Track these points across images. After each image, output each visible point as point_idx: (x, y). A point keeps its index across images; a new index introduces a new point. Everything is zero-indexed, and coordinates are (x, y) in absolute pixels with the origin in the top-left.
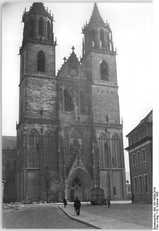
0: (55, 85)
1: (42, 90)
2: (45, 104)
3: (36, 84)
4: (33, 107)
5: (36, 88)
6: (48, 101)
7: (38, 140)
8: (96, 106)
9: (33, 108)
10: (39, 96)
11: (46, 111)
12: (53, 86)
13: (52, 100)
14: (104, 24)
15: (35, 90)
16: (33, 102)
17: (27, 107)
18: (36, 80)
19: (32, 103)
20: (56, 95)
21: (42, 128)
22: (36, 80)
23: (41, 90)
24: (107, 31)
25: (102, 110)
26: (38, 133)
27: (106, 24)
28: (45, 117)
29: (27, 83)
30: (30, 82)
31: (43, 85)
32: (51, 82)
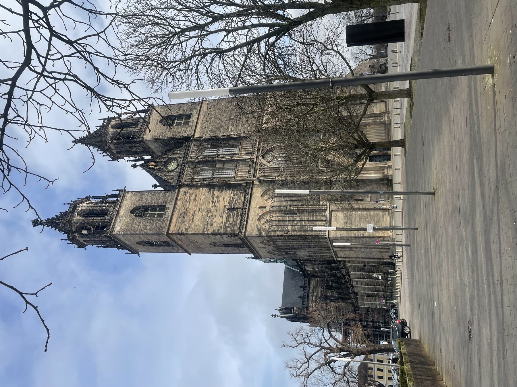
3: (184, 218)
6: (214, 201)
8: (229, 130)
9: (224, 222)
10: (205, 213)
11: (230, 202)
12: (191, 192)
13: (213, 193)
15: (193, 218)
16: (213, 222)
17: (220, 232)
19: (215, 225)
20: (204, 189)
26: (267, 213)
28: (239, 204)
29: (180, 232)
30: (179, 228)
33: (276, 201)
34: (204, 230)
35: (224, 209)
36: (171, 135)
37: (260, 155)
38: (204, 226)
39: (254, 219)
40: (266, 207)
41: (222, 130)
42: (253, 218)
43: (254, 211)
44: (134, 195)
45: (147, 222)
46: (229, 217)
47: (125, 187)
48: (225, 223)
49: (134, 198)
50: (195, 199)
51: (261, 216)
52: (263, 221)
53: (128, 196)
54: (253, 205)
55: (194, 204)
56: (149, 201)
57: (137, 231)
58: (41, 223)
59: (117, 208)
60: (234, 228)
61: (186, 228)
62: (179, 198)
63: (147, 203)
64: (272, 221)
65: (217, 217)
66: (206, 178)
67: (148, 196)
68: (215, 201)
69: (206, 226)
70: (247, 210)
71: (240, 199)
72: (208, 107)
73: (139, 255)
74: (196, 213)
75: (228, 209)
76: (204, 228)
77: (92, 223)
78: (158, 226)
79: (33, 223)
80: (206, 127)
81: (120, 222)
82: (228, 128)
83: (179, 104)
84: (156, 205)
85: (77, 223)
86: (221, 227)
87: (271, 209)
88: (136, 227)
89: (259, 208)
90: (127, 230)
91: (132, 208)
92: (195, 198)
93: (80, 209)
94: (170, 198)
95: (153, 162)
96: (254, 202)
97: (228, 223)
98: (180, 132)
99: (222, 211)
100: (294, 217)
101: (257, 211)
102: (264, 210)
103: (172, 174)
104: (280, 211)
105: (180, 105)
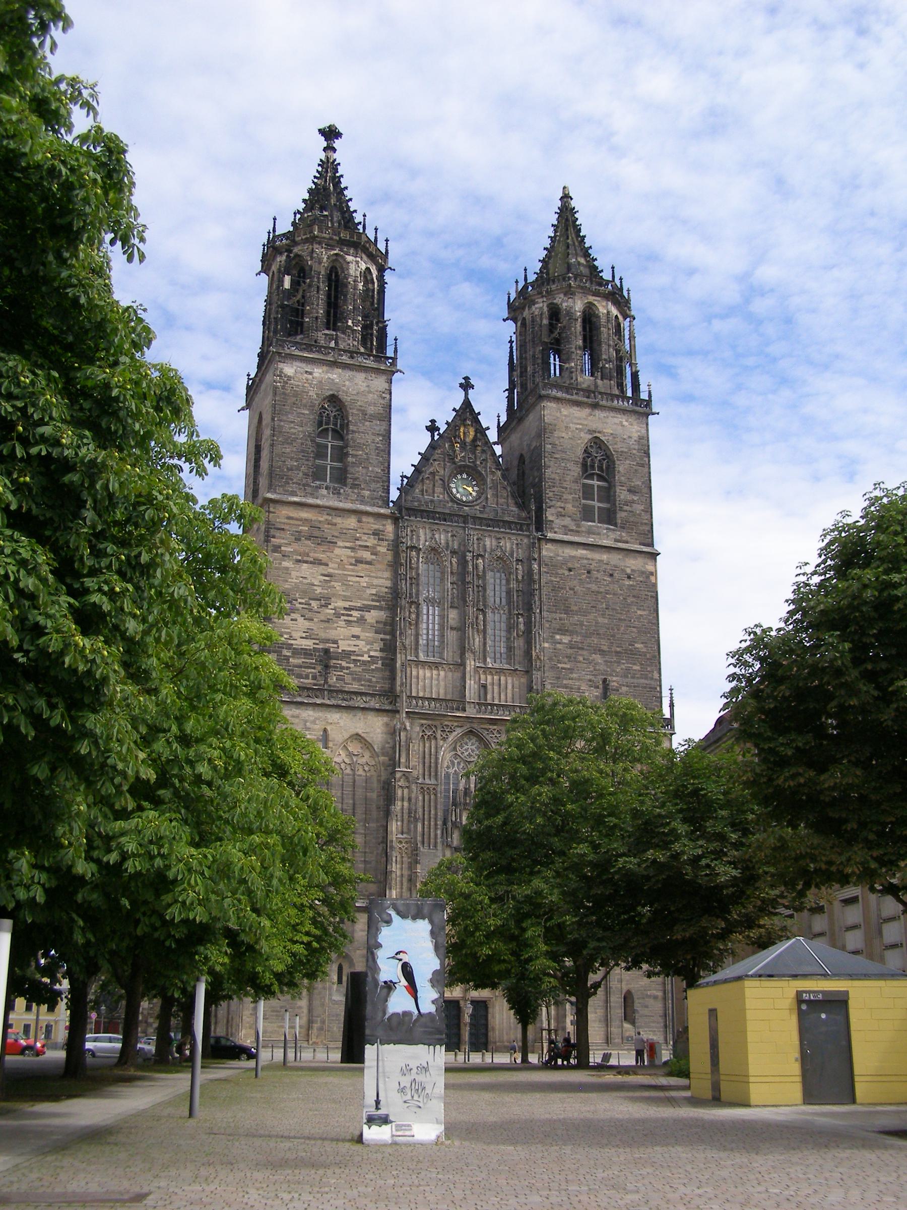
1: (331, 565)
2: (342, 623)
3: (309, 538)
4: (291, 638)
5: (308, 556)
6: (352, 613)
8: (558, 637)
9: (292, 642)
10: (319, 590)
11: (347, 655)
12: (379, 548)
13: (375, 608)
14: (602, 282)
15: (306, 562)
16: (294, 616)
18: (306, 520)
20: (388, 583)
21: (329, 728)
22: (305, 521)
23: (327, 565)
24: (615, 312)
25: (580, 652)
27: (608, 282)
29: (272, 532)
30: (283, 529)
35: (327, 641)
36: (553, 476)
37: (475, 726)
39: (296, 721)
41: (558, 616)
42: (297, 717)
43: (316, 719)
45: (302, 444)
46: (305, 654)
50: (359, 561)
53: (379, 383)
54: (334, 717)
55: (345, 562)
57: (281, 421)
58: (329, 148)
59: (345, 358)
61: (280, 547)
62: (364, 519)
65: (307, 624)
67: (373, 434)
68: (351, 616)
70: (319, 701)
72: (632, 570)
73: (243, 409)
74: (322, 569)
75: (326, 651)
79: (329, 127)
80: (570, 570)
81: (306, 372)
82: (563, 631)
90: (284, 394)
91: (345, 398)
92: (361, 562)
93: (349, 258)
94: (367, 493)
95: (476, 435)
97: (288, 654)
99: (323, 635)
102: (320, 745)
103: (438, 490)
105: (645, 490)
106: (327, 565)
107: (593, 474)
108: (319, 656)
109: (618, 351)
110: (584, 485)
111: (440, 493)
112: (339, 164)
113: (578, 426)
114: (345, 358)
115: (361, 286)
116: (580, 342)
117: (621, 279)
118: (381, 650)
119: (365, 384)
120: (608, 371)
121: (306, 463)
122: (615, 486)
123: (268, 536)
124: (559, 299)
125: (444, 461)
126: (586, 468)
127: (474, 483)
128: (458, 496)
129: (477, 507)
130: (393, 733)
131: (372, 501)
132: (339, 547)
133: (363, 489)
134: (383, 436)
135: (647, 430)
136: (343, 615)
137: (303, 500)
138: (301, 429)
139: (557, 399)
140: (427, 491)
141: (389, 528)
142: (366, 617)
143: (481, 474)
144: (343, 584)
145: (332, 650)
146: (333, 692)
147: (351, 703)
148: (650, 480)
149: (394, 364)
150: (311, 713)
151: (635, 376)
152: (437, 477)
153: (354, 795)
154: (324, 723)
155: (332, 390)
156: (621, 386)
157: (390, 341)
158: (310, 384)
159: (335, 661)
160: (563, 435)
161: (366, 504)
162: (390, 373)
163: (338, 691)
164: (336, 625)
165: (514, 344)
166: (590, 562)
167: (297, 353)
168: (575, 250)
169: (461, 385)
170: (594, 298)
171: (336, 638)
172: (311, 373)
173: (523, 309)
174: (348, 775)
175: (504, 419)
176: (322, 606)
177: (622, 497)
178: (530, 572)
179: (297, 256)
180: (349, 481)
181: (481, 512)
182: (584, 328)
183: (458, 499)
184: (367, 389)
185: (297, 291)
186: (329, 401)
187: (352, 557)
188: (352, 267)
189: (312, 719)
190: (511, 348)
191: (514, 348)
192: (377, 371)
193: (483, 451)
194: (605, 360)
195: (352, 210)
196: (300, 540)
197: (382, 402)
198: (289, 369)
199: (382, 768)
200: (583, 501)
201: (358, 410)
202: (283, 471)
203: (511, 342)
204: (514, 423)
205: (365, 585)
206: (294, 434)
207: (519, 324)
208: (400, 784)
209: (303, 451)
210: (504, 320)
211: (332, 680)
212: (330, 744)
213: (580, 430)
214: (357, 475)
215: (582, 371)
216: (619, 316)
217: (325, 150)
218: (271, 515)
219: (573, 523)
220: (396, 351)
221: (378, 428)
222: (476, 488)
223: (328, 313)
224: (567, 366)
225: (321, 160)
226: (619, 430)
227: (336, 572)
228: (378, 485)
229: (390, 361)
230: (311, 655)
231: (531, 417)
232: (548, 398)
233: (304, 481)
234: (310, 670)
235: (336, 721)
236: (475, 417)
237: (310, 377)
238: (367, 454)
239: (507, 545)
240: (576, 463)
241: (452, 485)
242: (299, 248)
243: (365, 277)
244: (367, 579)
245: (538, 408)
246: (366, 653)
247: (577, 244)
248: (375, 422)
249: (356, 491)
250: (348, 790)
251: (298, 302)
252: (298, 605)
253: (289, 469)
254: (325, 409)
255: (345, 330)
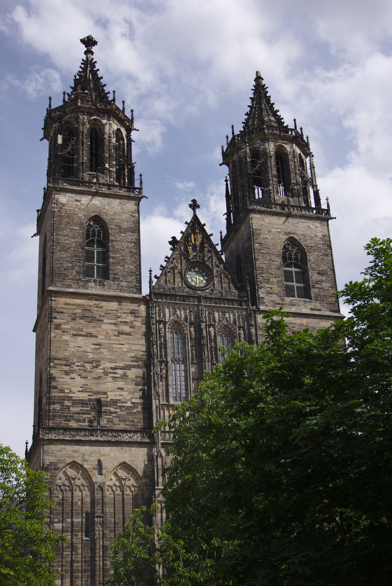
0: (140, 319)
1: (100, 337)
3: (83, 317)
5: (82, 330)
7: (88, 500)
10: (91, 356)
11: (114, 402)
12: (135, 323)
13: (134, 367)
14: (286, 129)
15: (81, 335)
16: (72, 375)
17: (53, 390)
18: (79, 305)
19: (67, 379)
20: (144, 348)
21: (102, 459)
23: (97, 337)
24: (298, 151)
27: (292, 130)
28: (110, 421)
29: (54, 315)
30: (62, 312)
31: (103, 321)
32: (129, 312)
33: (114, 494)
34: (56, 359)
35: (98, 393)
36: (261, 266)
38: (64, 359)
39: (77, 454)
40: (100, 473)
42: (77, 452)
43: (92, 452)
44: (132, 216)
45: (75, 251)
47: (145, 197)
48: (70, 399)
49: (124, 216)
50: (120, 333)
51: (82, 466)
52: (71, 472)
53: (131, 205)
55: (110, 333)
56: (117, 245)
57: (58, 235)
58: (88, 52)
59: (104, 190)
60: (60, 416)
61: (60, 325)
63: (115, 243)
64: (72, 491)
65: (83, 381)
66: (166, 348)
67: (127, 242)
68: (116, 373)
69: (64, 362)
70: (93, 438)
71: (120, 421)
73: (35, 235)
74: (93, 340)
75: (99, 401)
76: (60, 359)
77: (78, 149)
78: (66, 272)
79: (88, 37)
81: (76, 200)
83: (334, 270)
84: (111, 260)
85: (78, 122)
86: (62, 391)
87: (96, 486)
88: (66, 232)
89: (99, 461)
90: (60, 216)
91: (106, 218)
93: (104, 121)
94: (124, 284)
95: (203, 240)
96: (111, 451)
98: (268, 282)
99: (95, 389)
100: (80, 534)
101: (92, 458)
102: (96, 472)
103: (178, 280)
104: (93, 503)
105: (331, 273)
106: (97, 337)
107: (291, 263)
108: (93, 404)
109: (303, 177)
110: (285, 271)
111: (179, 282)
112: (96, 62)
113: (278, 230)
114: (104, 190)
115: (114, 140)
116: (275, 172)
117: (301, 129)
118: (140, 398)
119: (120, 207)
120: (296, 191)
121: (78, 264)
122: (308, 271)
123: (51, 318)
124: (258, 144)
125: (181, 259)
126: (286, 260)
127: (204, 274)
128: (193, 284)
129: (207, 291)
130: (151, 459)
131: (129, 289)
132: (105, 323)
133: (122, 281)
134: (135, 243)
135: (328, 231)
136: (110, 373)
137: (77, 290)
138: (73, 240)
139: (261, 212)
140: (169, 281)
141: (143, 308)
142: (128, 374)
143: (208, 267)
144: (109, 351)
145: (102, 399)
146: (103, 431)
147: (119, 439)
148: (333, 265)
149: (140, 192)
150: (87, 448)
151: (316, 194)
152: (176, 271)
153: (123, 510)
154: (98, 455)
155: (95, 212)
156: (307, 201)
157: (137, 177)
158: (79, 209)
159: (105, 408)
160: (267, 236)
161: (124, 291)
162: (138, 200)
163: (109, 431)
164: (105, 381)
165: (229, 182)
166: (294, 325)
167: (68, 187)
168: (267, 112)
169: (190, 206)
170: (283, 141)
171: (106, 391)
172: (79, 201)
173: (233, 155)
174: (118, 495)
175: (225, 233)
176: (94, 367)
177: (314, 278)
178: (250, 334)
179: (67, 122)
180: (111, 276)
181: (210, 294)
182: (277, 163)
183: (192, 286)
184: (121, 210)
185: (68, 145)
186: (93, 221)
187: (116, 330)
188: (107, 127)
189: (88, 452)
190: (227, 185)
191: (229, 185)
192: (129, 198)
193: (209, 251)
194: (294, 183)
195: (106, 92)
196: (75, 319)
197: (133, 219)
198: (63, 198)
199: (145, 488)
200: (285, 283)
201: (116, 225)
202: (61, 270)
203: (226, 181)
204: (232, 234)
205: (126, 350)
206: (69, 244)
207: (231, 166)
208: (159, 499)
209: (75, 256)
210: (220, 165)
211: (104, 422)
212: (104, 471)
213: (279, 232)
214: (117, 271)
215: (277, 192)
216: (301, 154)
217: (86, 53)
218: (53, 302)
219: (279, 298)
220: (141, 183)
221: (130, 238)
222: (206, 278)
223: (91, 160)
224: (266, 189)
225: (83, 60)
226: (308, 232)
227: (104, 341)
228: (133, 278)
229: (137, 190)
230: (87, 404)
231: (243, 227)
232: (254, 211)
233: (77, 277)
234: (86, 416)
235: (107, 453)
236: (202, 227)
237: (79, 204)
238: (123, 256)
239: (230, 316)
240: (278, 256)
241: (188, 276)
242: (68, 116)
243: (117, 135)
244: (127, 346)
245: (248, 218)
246: (129, 400)
247: (268, 108)
248: (128, 233)
249: (116, 283)
250: (119, 506)
251: (69, 153)
252: (75, 368)
253: (65, 269)
254: (91, 226)
255: (103, 171)
